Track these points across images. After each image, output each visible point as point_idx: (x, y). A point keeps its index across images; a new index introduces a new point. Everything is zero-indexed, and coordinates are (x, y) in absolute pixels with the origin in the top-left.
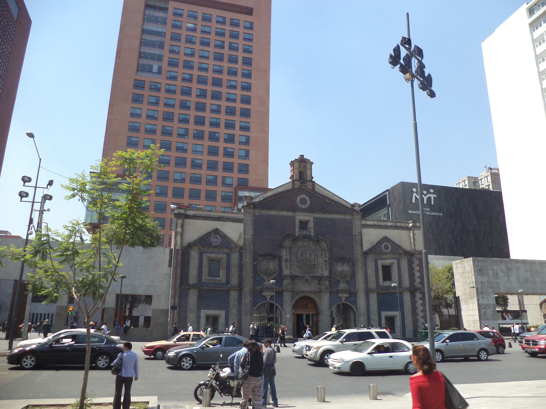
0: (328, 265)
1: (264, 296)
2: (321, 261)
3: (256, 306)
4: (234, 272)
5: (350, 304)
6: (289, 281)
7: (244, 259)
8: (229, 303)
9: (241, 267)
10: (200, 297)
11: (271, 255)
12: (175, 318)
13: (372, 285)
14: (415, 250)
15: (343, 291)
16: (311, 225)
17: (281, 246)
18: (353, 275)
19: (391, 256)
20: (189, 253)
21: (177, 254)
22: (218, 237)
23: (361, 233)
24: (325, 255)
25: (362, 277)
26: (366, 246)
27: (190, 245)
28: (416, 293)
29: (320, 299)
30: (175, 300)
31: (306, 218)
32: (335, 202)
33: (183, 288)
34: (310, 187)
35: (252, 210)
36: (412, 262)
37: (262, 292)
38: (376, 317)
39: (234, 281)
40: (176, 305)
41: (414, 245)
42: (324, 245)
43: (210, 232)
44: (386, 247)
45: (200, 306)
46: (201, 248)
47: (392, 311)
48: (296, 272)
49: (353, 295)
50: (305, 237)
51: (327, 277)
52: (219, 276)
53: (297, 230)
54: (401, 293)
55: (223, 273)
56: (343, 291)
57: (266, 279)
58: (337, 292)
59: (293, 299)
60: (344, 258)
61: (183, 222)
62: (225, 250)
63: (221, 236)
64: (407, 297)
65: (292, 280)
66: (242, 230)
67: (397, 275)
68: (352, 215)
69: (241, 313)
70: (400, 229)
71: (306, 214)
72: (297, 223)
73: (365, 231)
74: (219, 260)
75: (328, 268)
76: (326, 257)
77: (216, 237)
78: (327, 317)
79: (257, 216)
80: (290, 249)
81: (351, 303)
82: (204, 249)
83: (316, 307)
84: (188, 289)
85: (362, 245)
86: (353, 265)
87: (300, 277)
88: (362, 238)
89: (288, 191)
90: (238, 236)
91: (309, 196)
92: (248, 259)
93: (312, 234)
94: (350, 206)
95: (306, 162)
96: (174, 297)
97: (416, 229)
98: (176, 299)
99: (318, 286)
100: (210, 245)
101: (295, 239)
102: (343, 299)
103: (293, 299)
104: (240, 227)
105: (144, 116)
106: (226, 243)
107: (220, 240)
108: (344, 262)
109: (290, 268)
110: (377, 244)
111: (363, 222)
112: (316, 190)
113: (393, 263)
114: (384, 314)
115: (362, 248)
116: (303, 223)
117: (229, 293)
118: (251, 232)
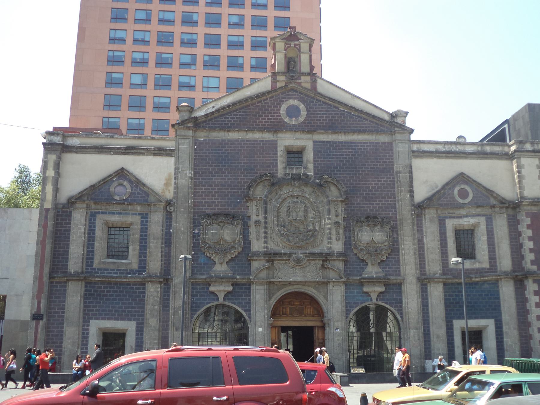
0: (341, 231)
1: (213, 293)
2: (326, 223)
4: (155, 248)
6: (263, 262)
7: (174, 224)
8: (143, 308)
9: (168, 240)
10: (89, 297)
11: (226, 215)
12: (39, 335)
14: (522, 198)
15: (373, 281)
16: (309, 156)
17: (248, 198)
18: (394, 249)
19: (473, 211)
20: (71, 216)
21: (46, 217)
22: (125, 183)
23: (411, 167)
25: (412, 252)
26: (421, 193)
27: (72, 202)
28: (526, 283)
29: (326, 297)
30: (39, 303)
32: (357, 110)
33: (57, 280)
34: (308, 86)
35: (190, 133)
36: (518, 222)
37: (210, 285)
38: (443, 332)
39: (155, 265)
40: (42, 311)
41: (520, 188)
42: (333, 192)
43: (110, 175)
44: (463, 194)
45: (89, 313)
46: (93, 206)
48: (277, 245)
49: (393, 288)
50: (296, 178)
51: (340, 254)
52: (126, 257)
53: (281, 166)
54: (496, 283)
55: (133, 251)
56: (373, 281)
57: (216, 260)
58: (361, 284)
59: (270, 298)
60: (375, 218)
61: (59, 158)
62: (139, 208)
63: (130, 182)
64: (507, 291)
65: (268, 261)
66: (172, 170)
67: (485, 247)
68: (392, 133)
69: (168, 326)
70: (491, 158)
71: (298, 135)
72: (279, 153)
74: (127, 227)
75: (342, 236)
76: (337, 216)
77: (122, 185)
78: (340, 331)
79: (201, 143)
80: (265, 202)
81: (391, 304)
82: (99, 207)
83: (320, 312)
84: (65, 282)
85: (411, 192)
86: (394, 229)
87: (285, 254)
88: (411, 178)
89: (263, 94)
90: (163, 182)
91: (304, 102)
92: (181, 223)
94: (387, 118)
95: (298, 39)
96: (37, 296)
97: (525, 156)
98: (42, 301)
99: (320, 272)
100: (109, 200)
101: (276, 184)
102: (374, 296)
103: (270, 298)
104: (168, 163)
105: (129, 41)
106: (141, 194)
107: (129, 190)
108: (375, 225)
109: (266, 237)
110: (444, 187)
112: (319, 89)
113: (476, 226)
114: (458, 325)
115: (412, 196)
116: (294, 152)
117: (144, 289)
118: (189, 173)
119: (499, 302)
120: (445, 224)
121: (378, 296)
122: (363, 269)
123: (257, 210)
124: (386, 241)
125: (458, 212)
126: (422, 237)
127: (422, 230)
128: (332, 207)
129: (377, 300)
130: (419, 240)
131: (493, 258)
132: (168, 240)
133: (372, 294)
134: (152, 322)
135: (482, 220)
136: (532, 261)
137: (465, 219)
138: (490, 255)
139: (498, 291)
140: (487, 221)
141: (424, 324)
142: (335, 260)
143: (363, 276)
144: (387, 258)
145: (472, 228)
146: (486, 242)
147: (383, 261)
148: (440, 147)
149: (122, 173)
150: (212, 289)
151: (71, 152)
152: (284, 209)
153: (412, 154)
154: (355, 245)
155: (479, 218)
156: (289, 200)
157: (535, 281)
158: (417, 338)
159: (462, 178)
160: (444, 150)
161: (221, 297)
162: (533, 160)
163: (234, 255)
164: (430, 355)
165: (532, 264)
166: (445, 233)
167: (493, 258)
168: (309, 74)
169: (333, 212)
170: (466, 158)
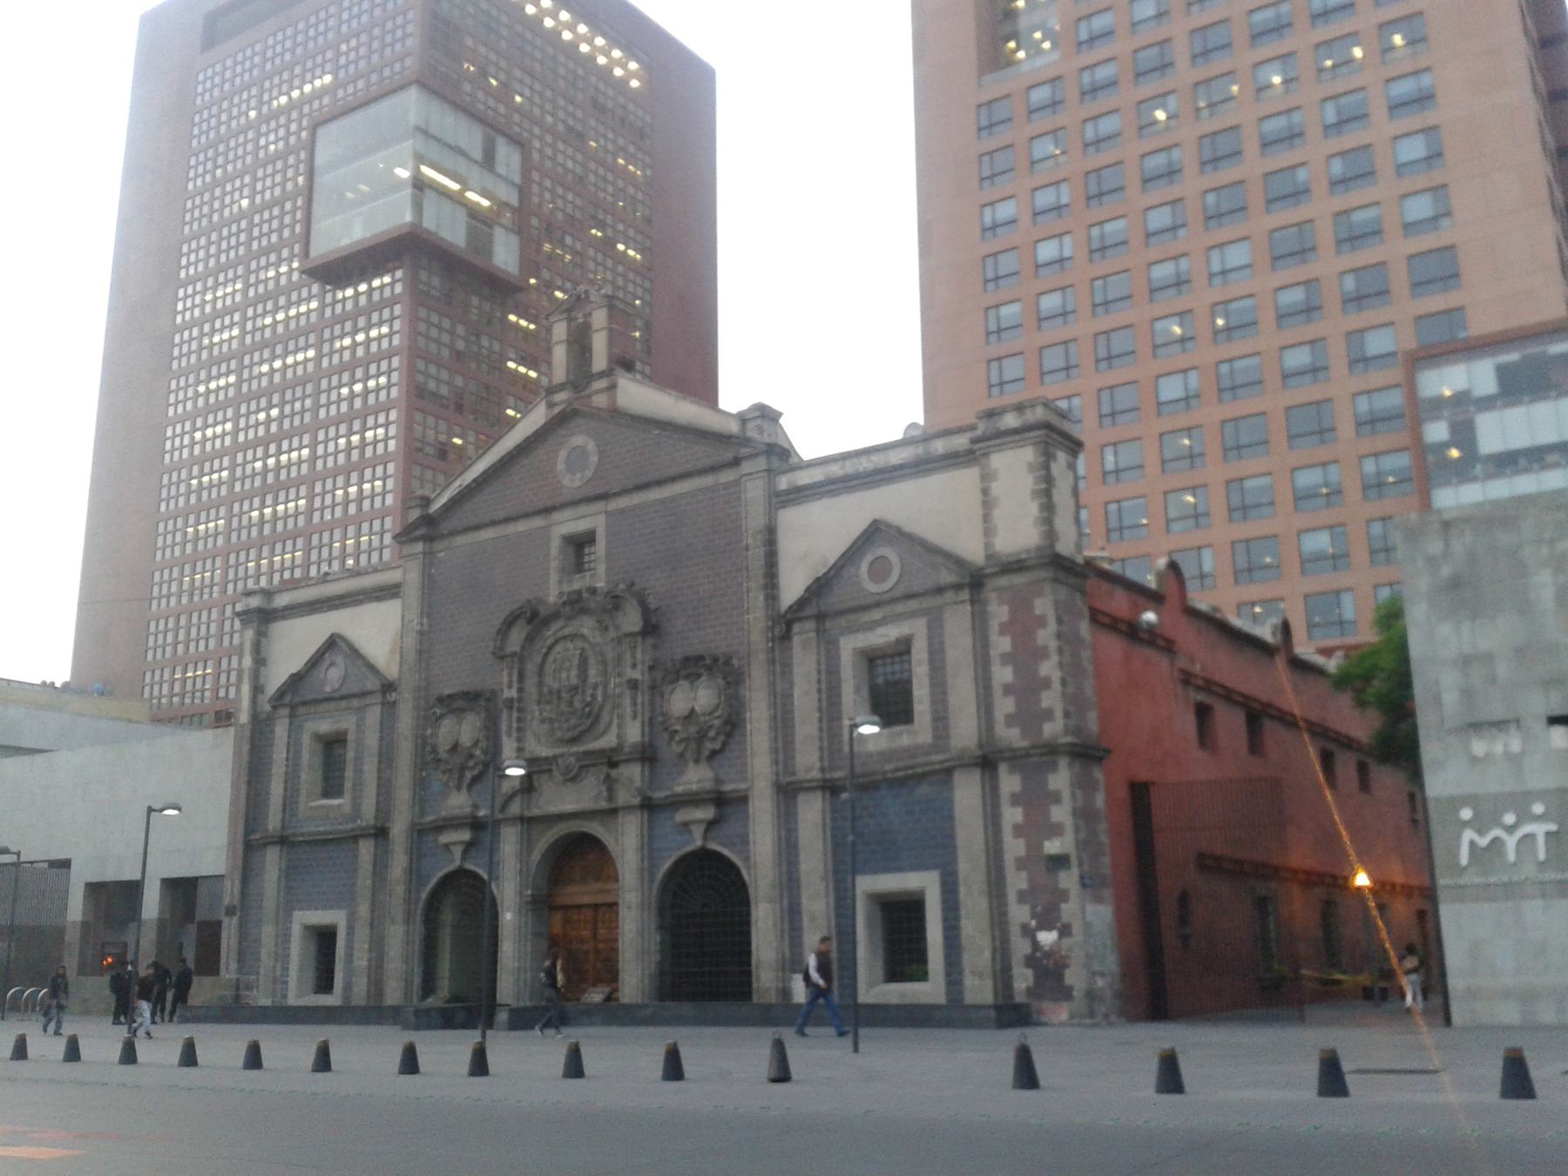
1: (447, 846)
5: (726, 852)
9: (386, 759)
10: (290, 873)
13: (808, 761)
16: (600, 547)
18: (733, 725)
19: (900, 608)
24: (634, 657)
26: (792, 587)
29: (616, 840)
31: (581, 526)
35: (419, 547)
44: (879, 570)
47: (900, 869)
62: (356, 703)
64: (967, 793)
71: (584, 509)
76: (634, 666)
87: (546, 759)
92: (405, 721)
94: (734, 428)
97: (1000, 448)
103: (530, 850)
119: (952, 828)
120: (838, 649)
121: (707, 830)
123: (510, 675)
124: (717, 707)
125: (865, 617)
129: (705, 838)
131: (941, 719)
135: (917, 629)
137: (881, 631)
142: (627, 761)
143: (679, 789)
144: (724, 744)
146: (926, 681)
147: (714, 753)
149: (333, 643)
152: (550, 667)
153: (774, 500)
154: (662, 723)
156: (558, 648)
157: (1012, 771)
159: (875, 532)
161: (457, 852)
163: (476, 772)
167: (941, 719)
168: (602, 375)
169: (628, 659)
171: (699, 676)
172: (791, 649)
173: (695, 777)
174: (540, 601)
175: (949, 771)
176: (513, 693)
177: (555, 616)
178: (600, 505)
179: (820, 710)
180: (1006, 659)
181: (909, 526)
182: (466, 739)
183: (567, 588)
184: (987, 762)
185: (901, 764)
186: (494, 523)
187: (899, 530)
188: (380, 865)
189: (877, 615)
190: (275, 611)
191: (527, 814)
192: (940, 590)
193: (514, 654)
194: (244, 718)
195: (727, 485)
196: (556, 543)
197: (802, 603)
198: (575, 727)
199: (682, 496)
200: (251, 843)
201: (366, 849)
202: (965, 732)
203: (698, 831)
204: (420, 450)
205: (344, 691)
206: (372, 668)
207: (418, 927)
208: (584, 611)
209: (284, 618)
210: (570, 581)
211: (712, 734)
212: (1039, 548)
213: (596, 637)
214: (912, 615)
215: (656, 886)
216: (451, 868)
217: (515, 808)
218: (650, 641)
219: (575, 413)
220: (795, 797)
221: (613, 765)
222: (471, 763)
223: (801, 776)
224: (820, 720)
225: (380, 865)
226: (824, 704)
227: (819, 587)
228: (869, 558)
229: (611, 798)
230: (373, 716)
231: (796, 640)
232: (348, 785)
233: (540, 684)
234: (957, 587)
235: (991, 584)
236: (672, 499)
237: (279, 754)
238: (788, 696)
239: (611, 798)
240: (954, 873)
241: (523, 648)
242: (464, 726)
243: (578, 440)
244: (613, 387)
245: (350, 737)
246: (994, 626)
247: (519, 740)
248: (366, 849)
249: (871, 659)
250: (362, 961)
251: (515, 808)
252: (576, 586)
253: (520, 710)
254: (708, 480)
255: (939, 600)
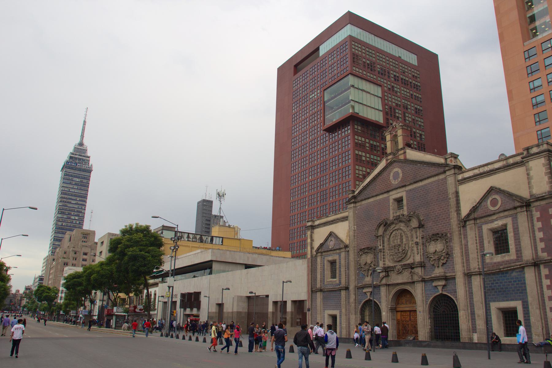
0: (420, 247)
1: (365, 293)
3: (360, 304)
5: (449, 295)
9: (348, 267)
10: (324, 299)
11: (368, 248)
15: (438, 279)
16: (405, 202)
17: (377, 237)
18: (449, 255)
19: (502, 215)
23: (457, 193)
25: (459, 255)
26: (465, 210)
31: (399, 195)
34: (402, 157)
35: (352, 205)
44: (494, 203)
45: (326, 306)
47: (507, 300)
53: (391, 212)
61: (312, 233)
62: (338, 251)
63: (335, 238)
64: (530, 275)
65: (385, 272)
71: (399, 190)
72: (391, 204)
73: (462, 188)
76: (417, 238)
80: (383, 237)
81: (451, 293)
90: (346, 235)
91: (400, 168)
93: (405, 213)
103: (389, 294)
111: (460, 177)
113: (506, 225)
119: (525, 287)
120: (482, 229)
121: (443, 288)
122: (434, 270)
125: (490, 218)
126: (467, 242)
127: (467, 237)
128: (413, 232)
129: (442, 291)
130: (465, 245)
132: (348, 267)
133: (438, 287)
134: (343, 310)
135: (509, 221)
136: (542, 249)
137: (496, 222)
138: (516, 248)
139: (524, 277)
140: (513, 221)
141: (471, 306)
142: (417, 267)
143: (433, 275)
144: (447, 261)
145: (504, 228)
146: (513, 238)
147: (443, 264)
148: (482, 170)
149: (331, 234)
150: (364, 291)
151: (316, 228)
152: (391, 239)
153: (457, 183)
155: (507, 219)
156: (394, 233)
158: (465, 317)
159: (492, 190)
160: (479, 172)
162: (539, 160)
164: (476, 330)
165: (542, 252)
166: (482, 237)
167: (519, 251)
168: (402, 149)
169: (415, 236)
170: (495, 173)
171: (438, 240)
172: (466, 230)
173: (438, 272)
174: (388, 219)
175: (523, 268)
176: (381, 247)
177: (392, 223)
178: (404, 189)
179: (477, 249)
180: (540, 230)
181: (502, 188)
182: (369, 261)
183: (395, 215)
184: (536, 264)
185: (506, 266)
186: (373, 197)
187: (499, 189)
188: (348, 298)
189: (494, 217)
190: (316, 226)
191: (388, 283)
192: (515, 208)
193: (381, 236)
194: (309, 256)
195: (442, 180)
196: (391, 201)
197: (468, 215)
198: (400, 257)
199: (429, 184)
200: (313, 291)
201: (343, 293)
202: (528, 255)
203: (440, 288)
204: (358, 177)
205: (335, 248)
206: (342, 241)
207: (359, 316)
208: (401, 221)
209: (318, 228)
210: (396, 213)
211: (442, 258)
212: (549, 192)
213: (405, 229)
214: (506, 217)
215: (428, 305)
216: (367, 299)
217: (384, 281)
218: (421, 230)
219: (395, 161)
220: (471, 277)
221: (412, 268)
222: (371, 268)
223: (472, 270)
224: (477, 252)
225: (348, 298)
226: (478, 247)
227: (474, 209)
228: (490, 199)
229: (412, 279)
230: (343, 255)
231: (468, 227)
232: (337, 275)
233: (389, 244)
234: (521, 207)
235: (532, 205)
236: (425, 185)
237: (319, 267)
238: (466, 245)
239: (412, 279)
240: (527, 302)
241: (383, 234)
242: (368, 257)
243: (396, 170)
244: (405, 153)
245: (337, 261)
246: (535, 219)
247: (384, 261)
248: (343, 293)
249: (495, 232)
250: (344, 325)
251: (384, 281)
252: (398, 214)
253: (384, 252)
254: (436, 178)
255: (515, 211)
